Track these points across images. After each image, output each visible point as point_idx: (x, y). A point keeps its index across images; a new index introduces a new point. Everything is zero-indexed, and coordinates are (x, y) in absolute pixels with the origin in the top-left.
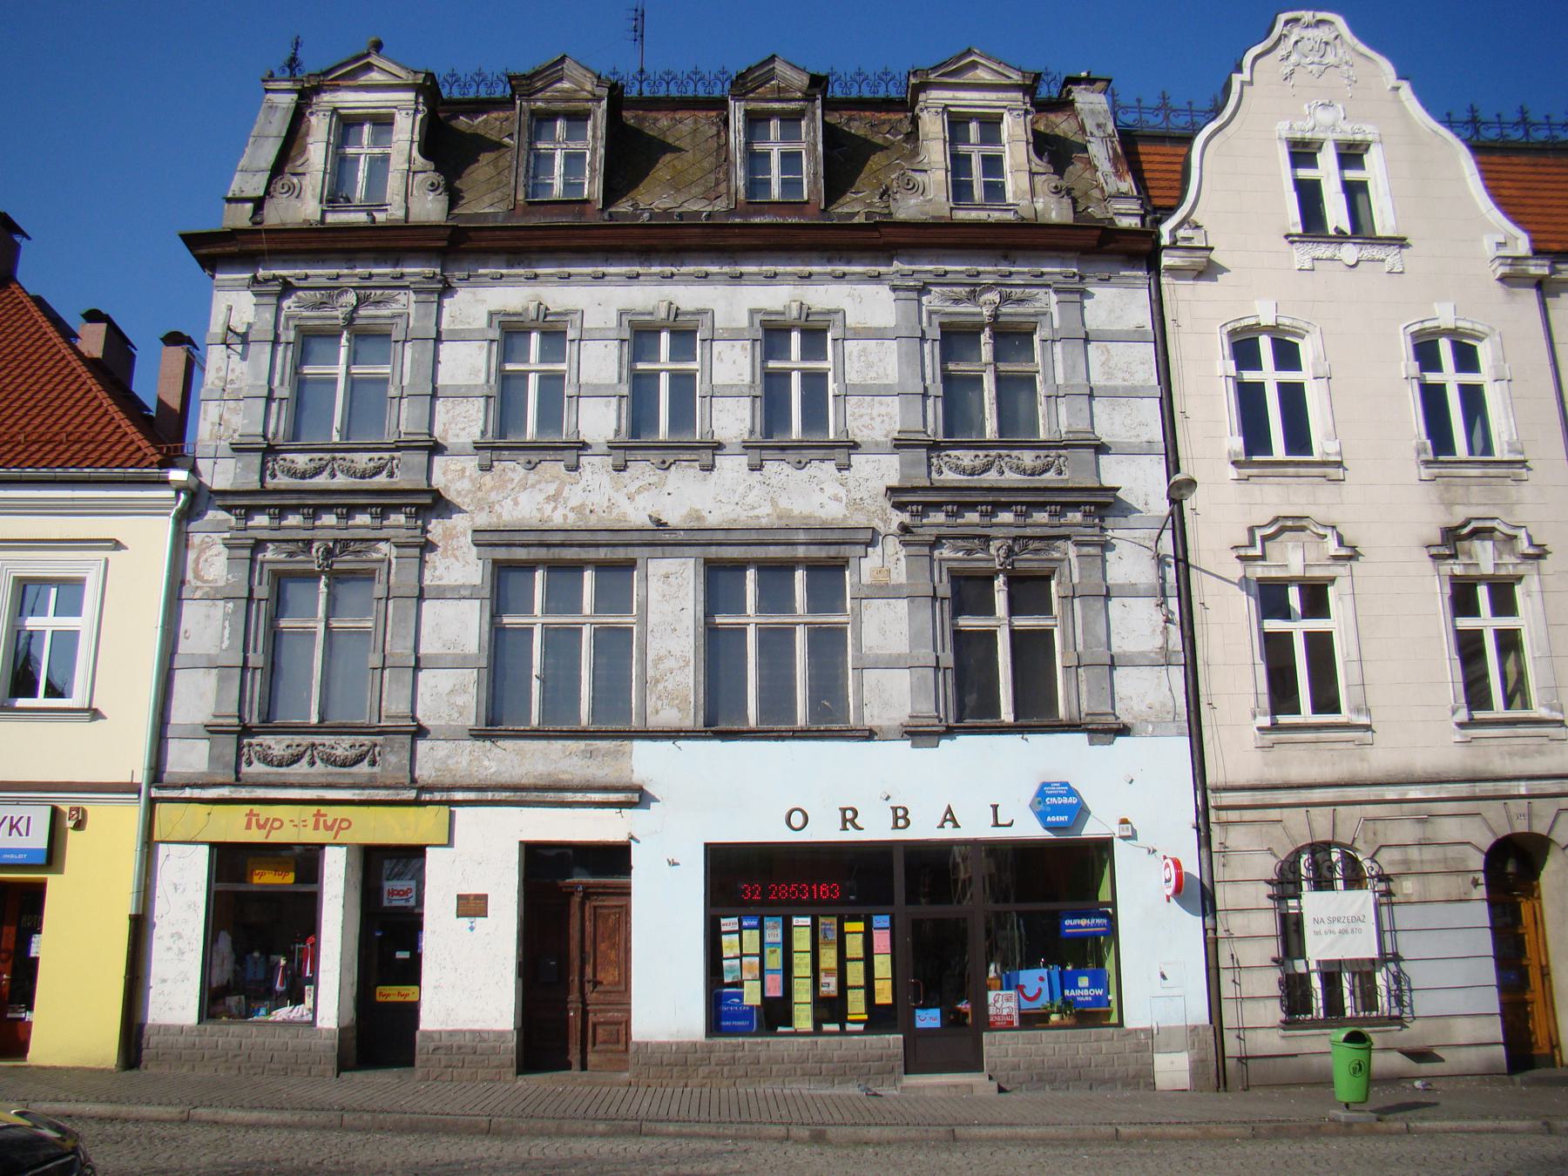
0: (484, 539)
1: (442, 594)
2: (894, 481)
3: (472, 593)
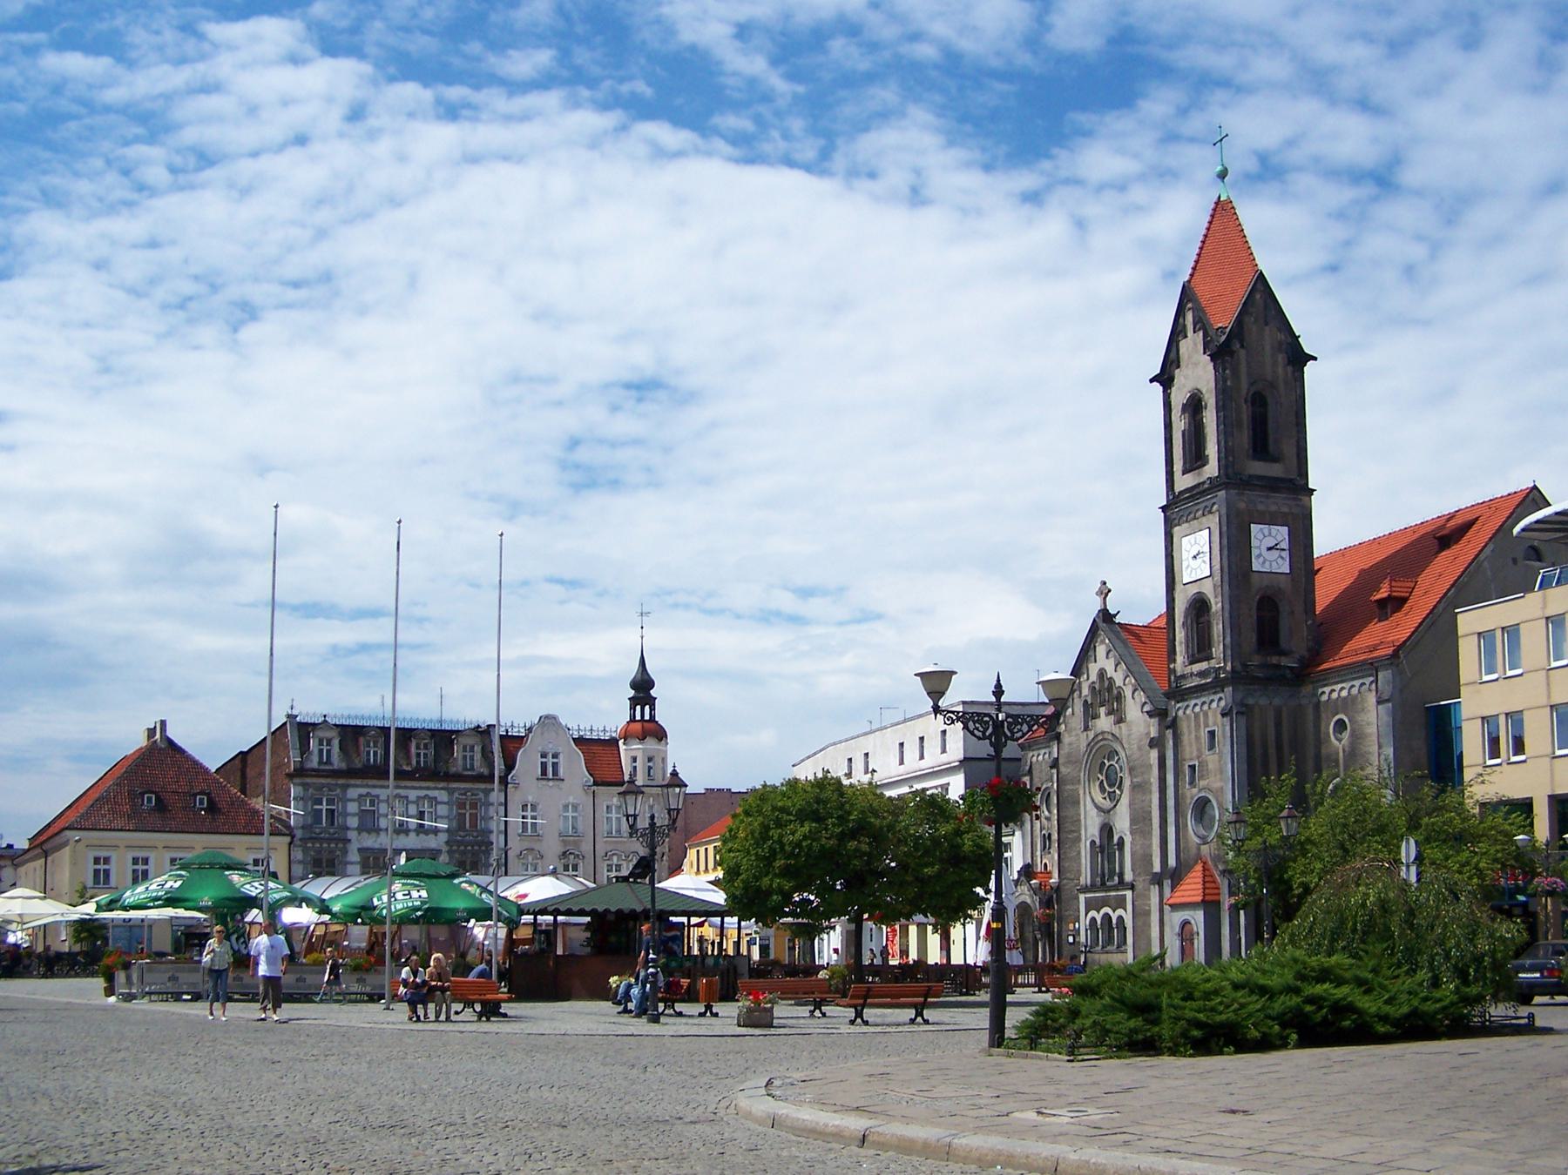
0: (360, 850)
1: (352, 863)
2: (445, 839)
3: (358, 863)
